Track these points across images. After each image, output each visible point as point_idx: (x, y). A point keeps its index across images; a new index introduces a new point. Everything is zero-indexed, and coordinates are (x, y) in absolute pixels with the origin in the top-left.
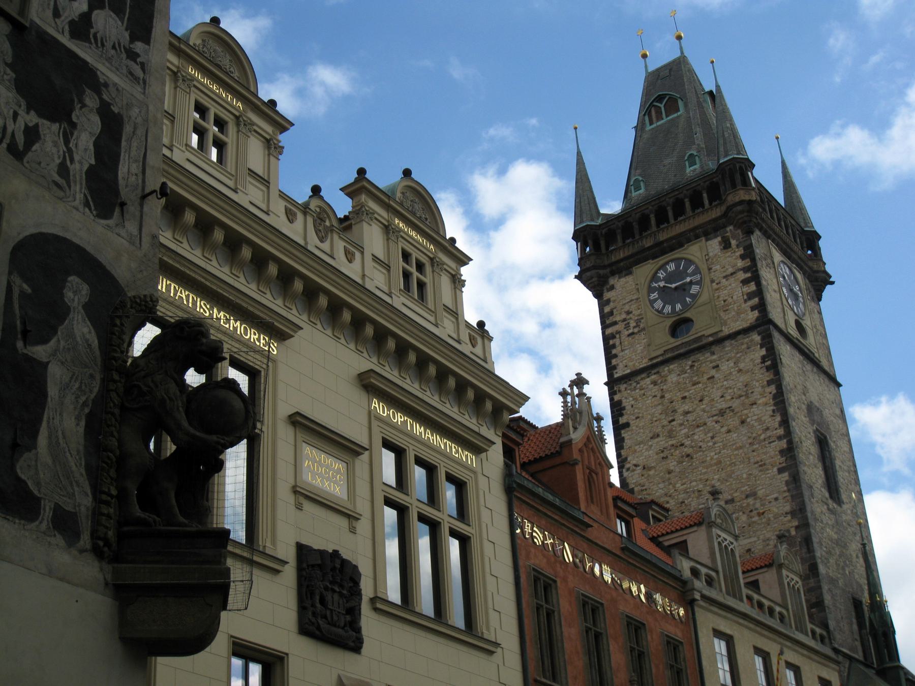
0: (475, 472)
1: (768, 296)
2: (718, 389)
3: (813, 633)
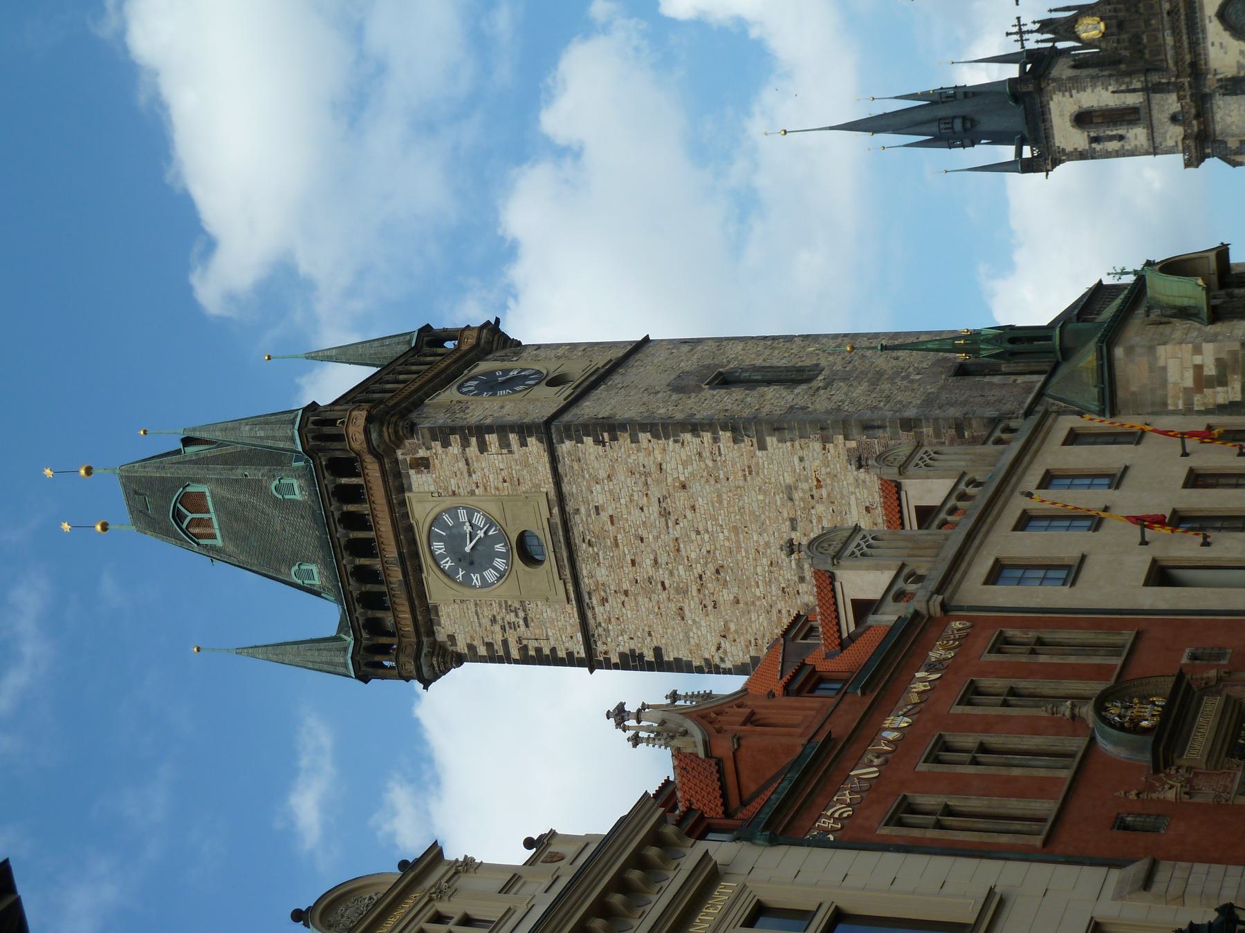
0: (745, 887)
1: (508, 418)
2: (629, 513)
3: (999, 441)
